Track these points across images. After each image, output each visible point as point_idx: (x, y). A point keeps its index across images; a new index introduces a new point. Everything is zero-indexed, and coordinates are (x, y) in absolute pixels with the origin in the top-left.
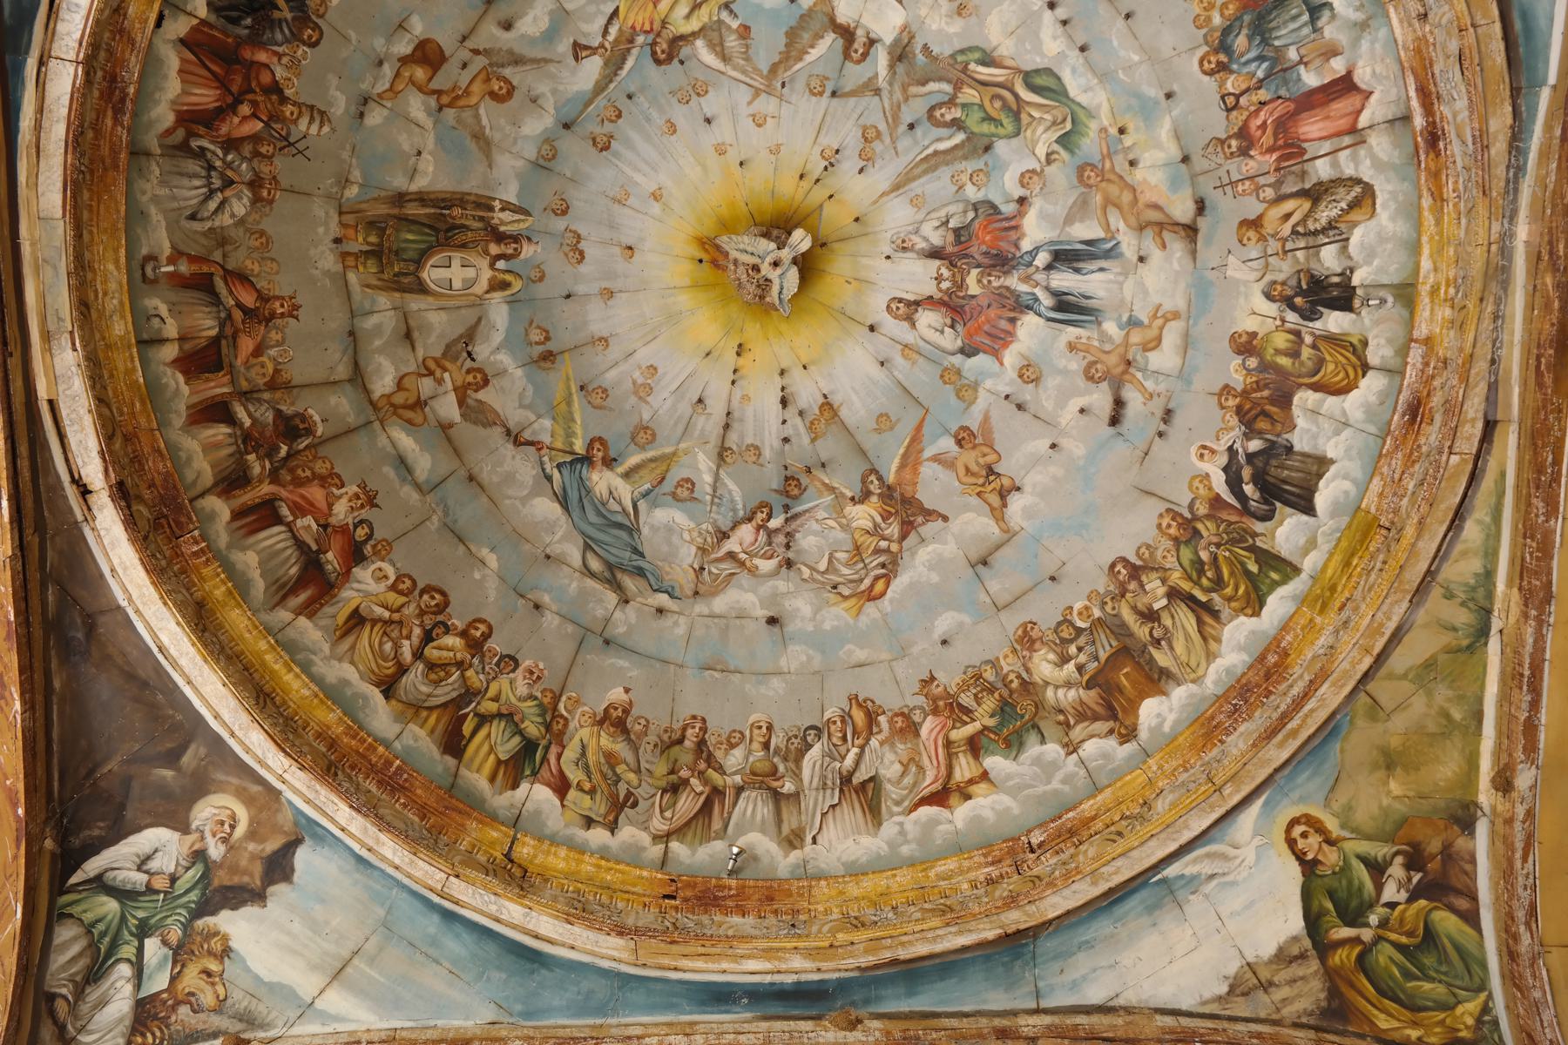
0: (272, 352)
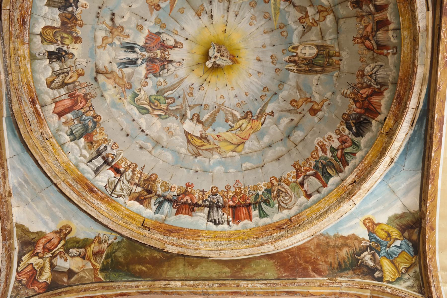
0: (361, 27)
